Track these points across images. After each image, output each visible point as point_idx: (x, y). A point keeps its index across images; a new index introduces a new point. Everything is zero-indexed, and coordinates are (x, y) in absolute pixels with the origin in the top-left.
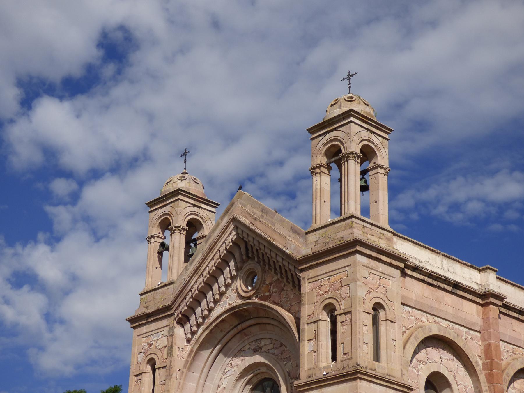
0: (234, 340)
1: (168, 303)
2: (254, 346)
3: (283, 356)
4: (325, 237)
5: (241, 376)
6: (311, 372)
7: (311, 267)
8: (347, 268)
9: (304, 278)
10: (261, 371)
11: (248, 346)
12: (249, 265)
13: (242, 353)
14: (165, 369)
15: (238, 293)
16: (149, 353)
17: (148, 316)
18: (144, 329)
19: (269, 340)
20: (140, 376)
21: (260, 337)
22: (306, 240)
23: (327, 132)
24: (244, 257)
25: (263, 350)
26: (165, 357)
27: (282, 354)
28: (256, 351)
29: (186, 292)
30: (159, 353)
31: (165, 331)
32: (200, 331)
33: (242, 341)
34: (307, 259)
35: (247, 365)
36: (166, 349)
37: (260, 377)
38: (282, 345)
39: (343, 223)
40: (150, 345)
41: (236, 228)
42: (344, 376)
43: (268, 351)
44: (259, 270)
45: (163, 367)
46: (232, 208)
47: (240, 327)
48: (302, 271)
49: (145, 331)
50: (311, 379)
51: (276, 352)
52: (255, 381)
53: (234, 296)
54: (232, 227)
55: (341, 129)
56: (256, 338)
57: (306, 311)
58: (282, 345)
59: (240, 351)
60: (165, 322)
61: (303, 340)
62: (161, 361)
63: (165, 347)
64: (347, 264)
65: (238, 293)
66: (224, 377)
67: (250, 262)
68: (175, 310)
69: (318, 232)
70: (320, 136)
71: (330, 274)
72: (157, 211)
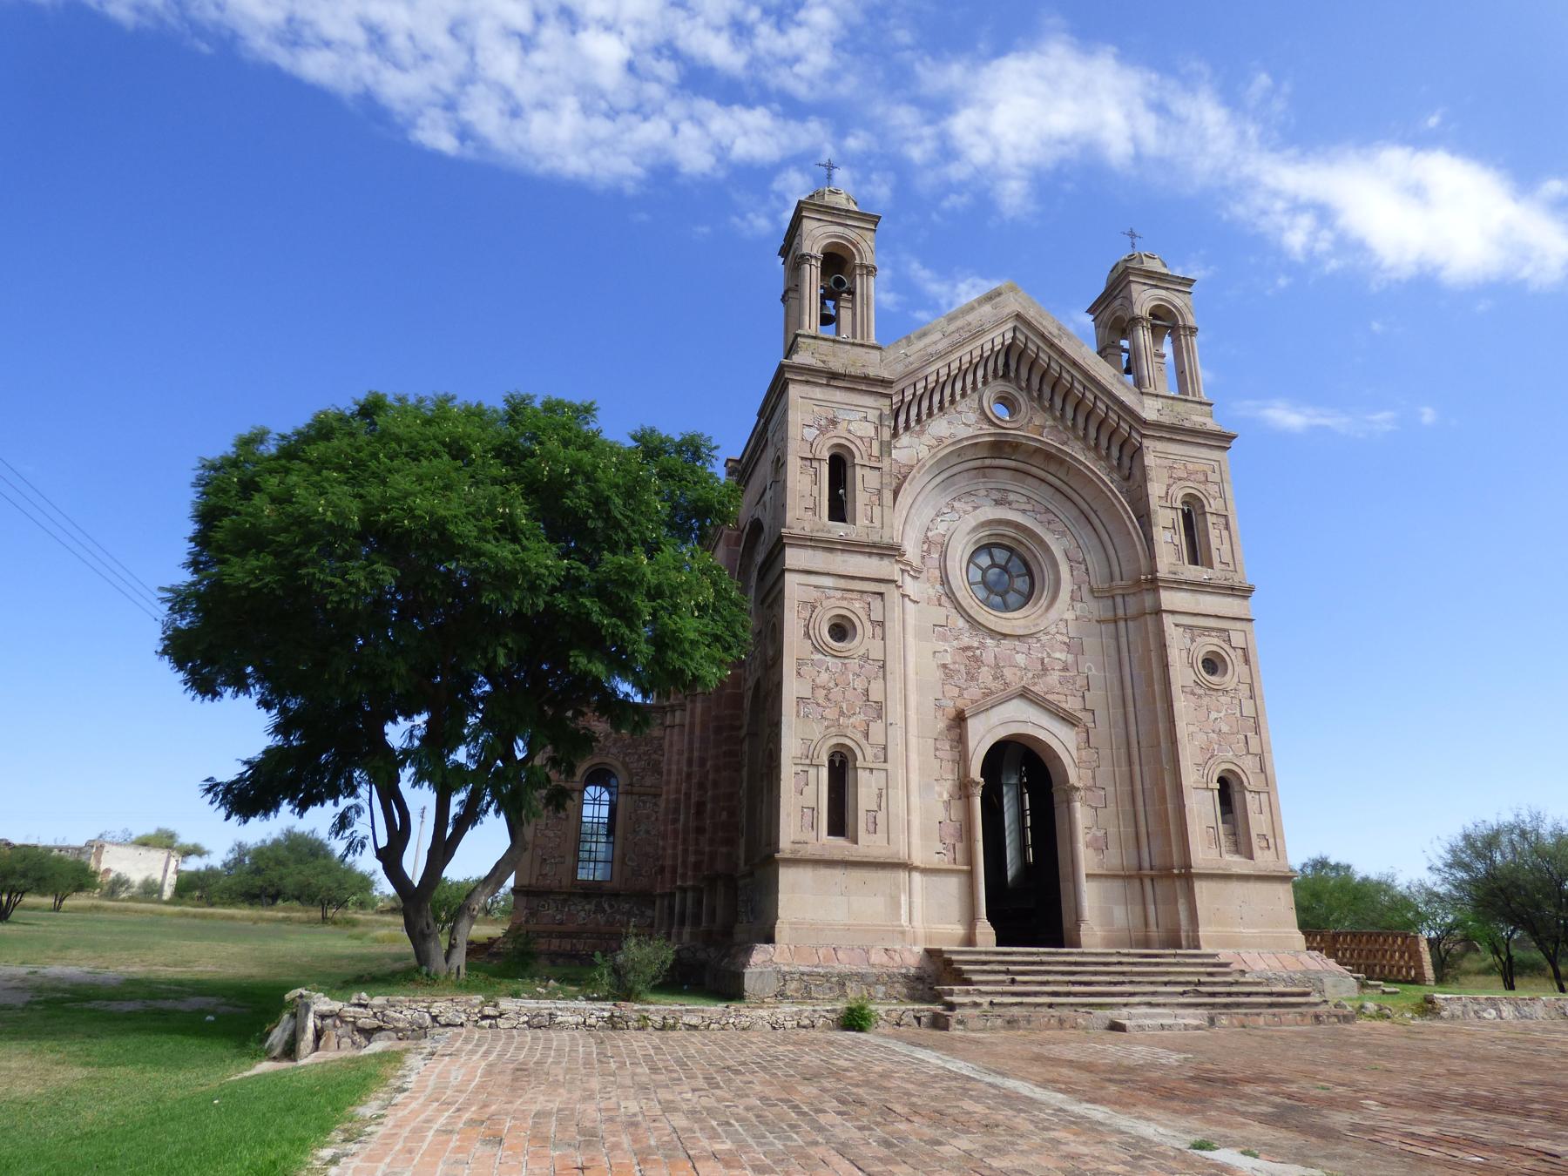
0: (965, 474)
1: (886, 375)
2: (996, 495)
3: (1051, 526)
4: (1172, 411)
5: (975, 529)
6: (1173, 569)
7: (1160, 438)
8: (1213, 463)
9: (1148, 448)
10: (1007, 533)
11: (983, 492)
12: (998, 387)
13: (973, 498)
14: (877, 473)
15: (983, 412)
16: (833, 434)
17: (834, 376)
18: (818, 393)
19: (1025, 499)
20: (815, 464)
21: (1008, 487)
22: (1141, 402)
23: (1156, 287)
24: (1001, 373)
25: (1014, 506)
26: (876, 452)
27: (1049, 523)
28: (998, 503)
29: (921, 376)
30: (858, 442)
31: (873, 415)
32: (905, 439)
33: (976, 481)
34: (1158, 426)
35: (991, 517)
36: (876, 445)
37: (993, 540)
38: (1048, 510)
39: (1198, 406)
40: (833, 422)
41: (1015, 329)
42: (1233, 589)
43: (1024, 511)
44: (1022, 398)
45: (871, 467)
46: (998, 299)
47: (988, 462)
48: (1143, 436)
49: (819, 396)
50: (1173, 576)
51: (1038, 516)
52: (985, 541)
53: (972, 417)
54: (1010, 325)
55: (1177, 293)
56: (999, 486)
57: (1155, 489)
58: (1048, 510)
59: (969, 493)
60: (869, 401)
61: (1157, 526)
62: (865, 456)
63: (871, 439)
64: (1213, 458)
65: (983, 412)
66: (939, 519)
67: (1000, 381)
68: (896, 393)
69: (1160, 400)
70: (1145, 284)
71: (1187, 459)
72: (821, 224)
